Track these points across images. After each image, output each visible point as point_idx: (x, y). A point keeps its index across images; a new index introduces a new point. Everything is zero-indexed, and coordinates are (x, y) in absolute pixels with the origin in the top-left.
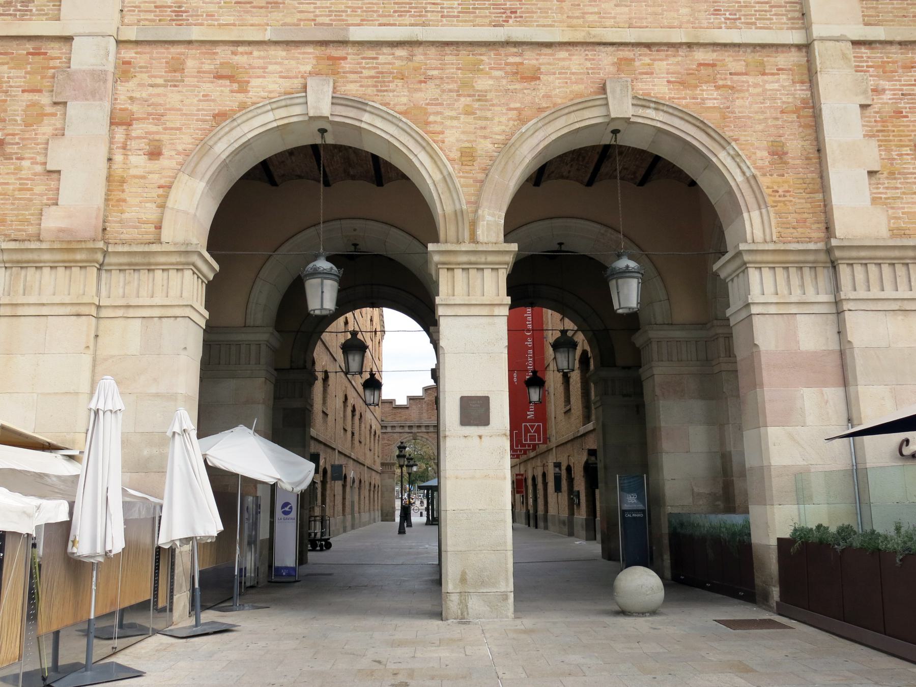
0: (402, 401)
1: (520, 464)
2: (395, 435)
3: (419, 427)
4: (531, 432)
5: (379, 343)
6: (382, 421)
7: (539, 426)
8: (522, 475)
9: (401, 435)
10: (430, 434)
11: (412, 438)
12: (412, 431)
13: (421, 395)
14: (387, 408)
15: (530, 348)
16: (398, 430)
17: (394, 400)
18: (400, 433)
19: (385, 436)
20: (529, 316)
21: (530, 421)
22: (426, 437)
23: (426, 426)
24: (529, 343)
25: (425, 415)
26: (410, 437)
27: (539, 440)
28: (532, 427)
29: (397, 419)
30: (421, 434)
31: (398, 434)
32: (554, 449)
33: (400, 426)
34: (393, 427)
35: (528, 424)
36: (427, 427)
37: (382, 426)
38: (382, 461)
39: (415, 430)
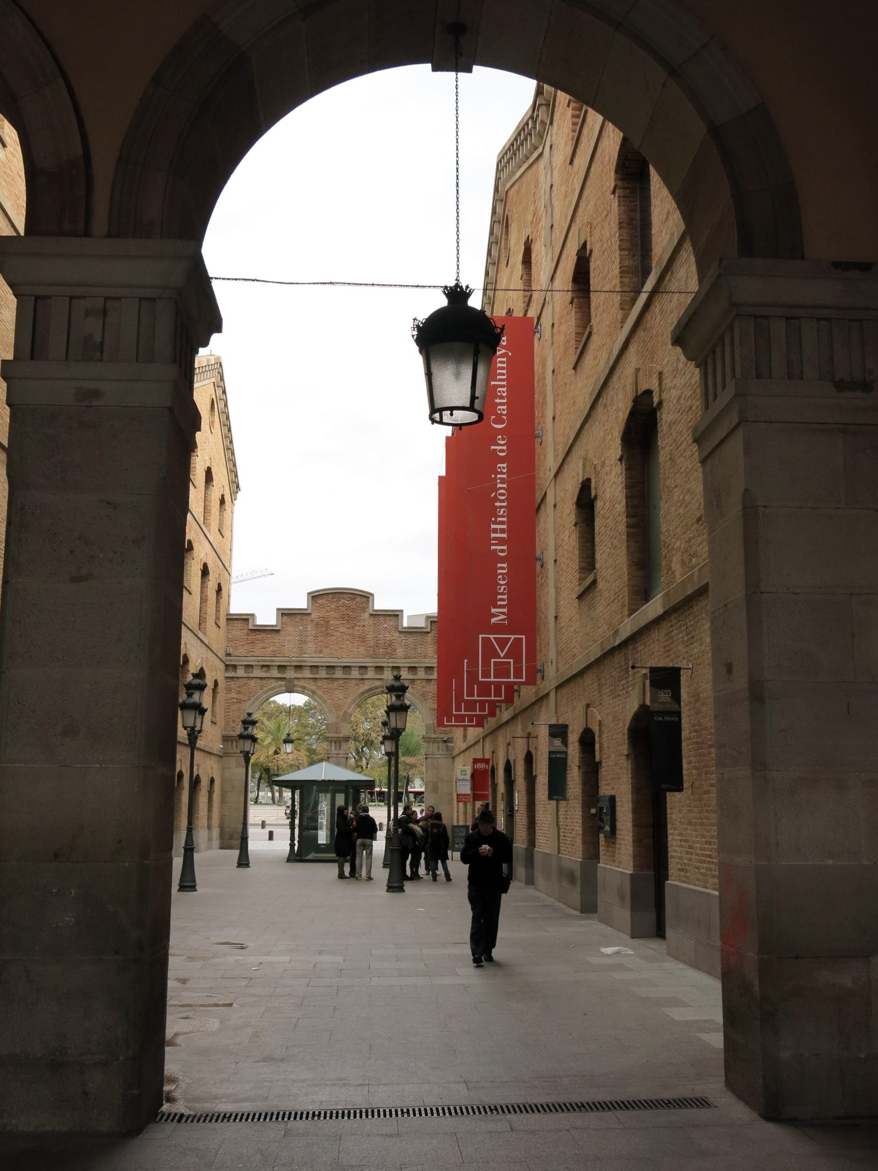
0: (267, 618)
1: (484, 738)
2: (252, 683)
3: (298, 668)
4: (500, 657)
5: (222, 501)
6: (229, 655)
8: (486, 761)
9: (265, 682)
10: (320, 683)
12: (285, 676)
13: (305, 607)
14: (238, 631)
15: (502, 460)
16: (257, 673)
17: (253, 615)
18: (261, 678)
19: (233, 684)
20: (503, 386)
21: (498, 628)
22: (313, 688)
23: (312, 666)
24: (500, 447)
25: (311, 646)
27: (518, 674)
28: (502, 643)
30: (302, 683)
31: (259, 681)
32: (552, 695)
33: (263, 666)
34: (248, 667)
35: (491, 636)
36: (314, 668)
37: (227, 666)
38: (227, 733)
39: (290, 674)
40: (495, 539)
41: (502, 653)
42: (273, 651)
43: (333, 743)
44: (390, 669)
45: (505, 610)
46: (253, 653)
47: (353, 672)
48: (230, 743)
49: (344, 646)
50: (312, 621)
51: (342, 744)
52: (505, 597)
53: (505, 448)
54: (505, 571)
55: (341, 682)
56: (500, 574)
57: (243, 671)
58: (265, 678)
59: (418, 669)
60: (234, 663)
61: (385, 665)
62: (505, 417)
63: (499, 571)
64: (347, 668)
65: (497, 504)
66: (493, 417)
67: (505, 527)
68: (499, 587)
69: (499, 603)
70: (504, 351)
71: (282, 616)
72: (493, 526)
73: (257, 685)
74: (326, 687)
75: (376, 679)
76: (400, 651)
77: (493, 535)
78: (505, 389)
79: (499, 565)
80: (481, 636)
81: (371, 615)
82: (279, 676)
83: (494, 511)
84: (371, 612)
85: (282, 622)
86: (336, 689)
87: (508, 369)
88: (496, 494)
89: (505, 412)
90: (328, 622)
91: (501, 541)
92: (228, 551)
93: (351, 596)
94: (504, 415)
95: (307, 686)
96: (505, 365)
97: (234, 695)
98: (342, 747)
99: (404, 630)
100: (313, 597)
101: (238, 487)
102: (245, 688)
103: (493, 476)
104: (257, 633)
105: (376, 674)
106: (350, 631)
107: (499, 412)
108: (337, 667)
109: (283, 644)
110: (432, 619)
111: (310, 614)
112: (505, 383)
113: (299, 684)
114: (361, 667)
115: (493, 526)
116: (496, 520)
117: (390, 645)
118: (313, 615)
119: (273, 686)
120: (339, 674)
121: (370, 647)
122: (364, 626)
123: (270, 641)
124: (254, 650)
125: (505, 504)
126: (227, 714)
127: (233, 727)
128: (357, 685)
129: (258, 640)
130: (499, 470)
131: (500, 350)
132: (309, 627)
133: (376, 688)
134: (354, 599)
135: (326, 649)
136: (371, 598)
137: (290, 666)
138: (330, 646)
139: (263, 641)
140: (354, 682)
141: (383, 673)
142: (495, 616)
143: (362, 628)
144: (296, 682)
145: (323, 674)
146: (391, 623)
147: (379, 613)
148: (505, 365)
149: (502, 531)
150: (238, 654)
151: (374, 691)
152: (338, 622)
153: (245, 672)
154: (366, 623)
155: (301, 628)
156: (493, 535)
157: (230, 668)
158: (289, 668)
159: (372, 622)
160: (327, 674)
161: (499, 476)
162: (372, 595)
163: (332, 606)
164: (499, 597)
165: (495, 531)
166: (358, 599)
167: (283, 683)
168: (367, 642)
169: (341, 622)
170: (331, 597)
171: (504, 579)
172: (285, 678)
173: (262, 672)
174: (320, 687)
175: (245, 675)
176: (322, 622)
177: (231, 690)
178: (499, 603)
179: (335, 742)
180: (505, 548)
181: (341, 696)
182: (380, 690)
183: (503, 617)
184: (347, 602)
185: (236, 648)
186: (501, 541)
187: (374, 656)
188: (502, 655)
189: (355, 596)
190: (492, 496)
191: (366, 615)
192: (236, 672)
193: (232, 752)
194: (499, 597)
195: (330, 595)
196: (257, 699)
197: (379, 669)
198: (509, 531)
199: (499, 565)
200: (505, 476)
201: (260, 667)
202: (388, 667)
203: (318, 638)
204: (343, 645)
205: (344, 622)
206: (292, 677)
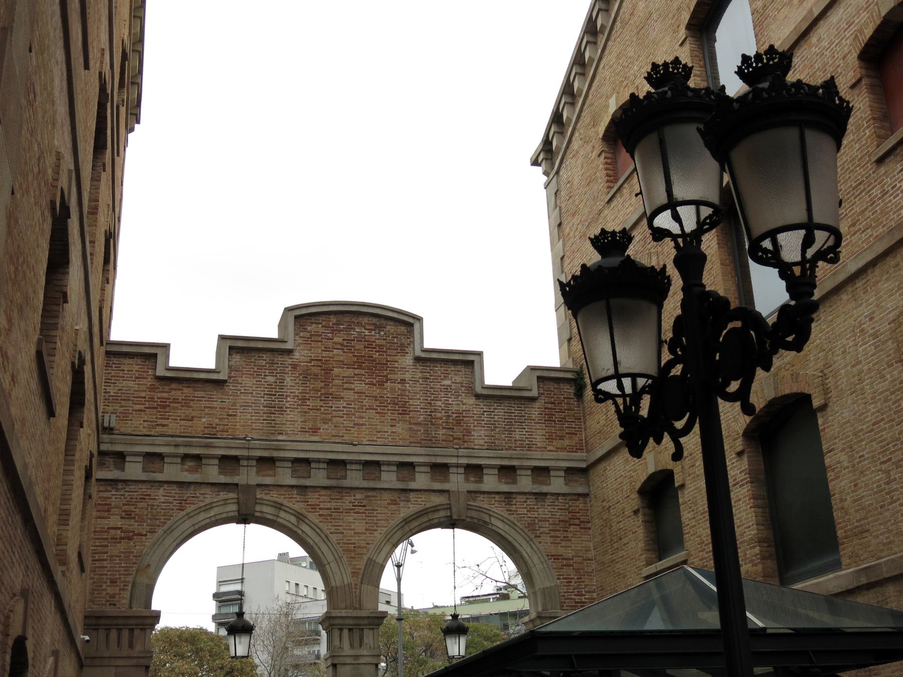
2: (160, 494)
9: (188, 493)
10: (313, 497)
11: (234, 507)
12: (236, 480)
16: (172, 471)
17: (166, 347)
18: (181, 484)
19: (114, 497)
22: (299, 507)
26: (225, 502)
29: (173, 427)
30: (274, 496)
31: (175, 490)
33: (185, 457)
36: (302, 463)
39: (248, 476)
42: (210, 426)
43: (346, 632)
44: (462, 470)
46: (165, 429)
47: (384, 476)
48: (102, 634)
49: (361, 421)
50: (295, 367)
51: (366, 632)
55: (358, 496)
57: (139, 467)
58: (190, 484)
59: (518, 472)
60: (118, 448)
61: (453, 461)
64: (372, 466)
71: (230, 354)
73: (171, 499)
74: (328, 505)
75: (434, 491)
76: (479, 436)
81: (418, 359)
82: (222, 479)
84: (418, 353)
85: (230, 367)
86: (348, 511)
90: (328, 371)
93: (375, 320)
95: (285, 502)
97: (115, 521)
98: (365, 640)
99: (485, 392)
100: (296, 317)
102: (143, 505)
104: (174, 386)
105: (433, 479)
106: (376, 391)
108: (352, 462)
109: (231, 412)
110: (540, 373)
111: (290, 352)
113: (267, 497)
114: (401, 465)
117: (458, 422)
118: (297, 355)
119: (208, 501)
120: (354, 478)
121: (418, 424)
122: (403, 381)
123: (204, 403)
124: (165, 422)
126: (98, 564)
127: (113, 596)
128: (394, 502)
129: (175, 401)
132: (288, 380)
133: (435, 509)
134: (379, 328)
135: (326, 426)
136: (417, 326)
137: (248, 458)
138: (335, 420)
139: (186, 403)
140: (387, 496)
141: (446, 479)
143: (400, 386)
144: (259, 494)
145: (319, 477)
146: (458, 379)
147: (435, 356)
150: (129, 431)
151: (431, 516)
152: (349, 372)
153: (144, 470)
154: (407, 376)
155: (271, 379)
157: (110, 461)
158: (244, 463)
159: (420, 375)
160: (329, 478)
162: (419, 319)
163: (336, 339)
166: (390, 328)
167: (232, 495)
168: (411, 414)
169: (357, 371)
170: (335, 321)
172: (237, 485)
173: (182, 470)
174: (314, 508)
175: (144, 477)
176: (316, 370)
177: (109, 511)
179: (350, 630)
181: (360, 526)
182: (442, 514)
184: (367, 333)
185: (124, 416)
187: (429, 442)
189: (383, 322)
191: (408, 360)
192: (123, 469)
193: (107, 654)
195: (332, 317)
196: (171, 530)
197: (440, 469)
201: (179, 460)
202: (458, 466)
203: (308, 403)
204: (362, 418)
205: (363, 372)
206: (250, 483)
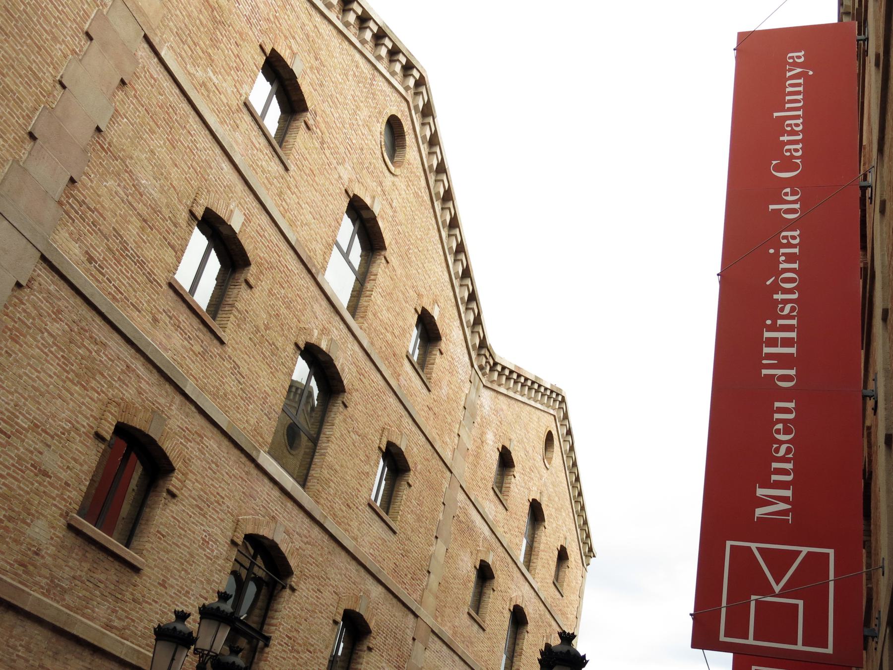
4: (771, 592)
5: (563, 555)
7: (816, 563)
15: (791, 225)
20: (797, 117)
27: (815, 635)
28: (780, 563)
35: (754, 546)
40: (769, 356)
41: (777, 583)
45: (788, 493)
52: (789, 466)
53: (797, 206)
54: (791, 416)
56: (779, 421)
62: (798, 161)
63: (777, 416)
65: (779, 296)
66: (774, 162)
67: (793, 335)
68: (775, 446)
69: (774, 477)
70: (799, 70)
72: (767, 335)
77: (766, 350)
78: (800, 121)
79: (777, 404)
80: (729, 543)
83: (772, 310)
87: (805, 93)
88: (776, 281)
89: (799, 154)
91: (783, 361)
92: (572, 617)
94: (797, 158)
96: (801, 89)
101: (591, 550)
103: (772, 251)
107: (788, 154)
112: (800, 113)
115: (767, 335)
116: (774, 322)
125: (795, 296)
130: (785, 241)
131: (790, 70)
142: (764, 503)
148: (801, 89)
149: (787, 342)
156: (766, 350)
161: (782, 251)
164: (775, 465)
165: (772, 342)
171: (787, 431)
178: (774, 477)
180: (792, 372)
183: (783, 506)
186: (783, 361)
188: (777, 588)
190: (768, 283)
194: (775, 465)
198: (800, 342)
199: (777, 404)
200: (796, 250)
